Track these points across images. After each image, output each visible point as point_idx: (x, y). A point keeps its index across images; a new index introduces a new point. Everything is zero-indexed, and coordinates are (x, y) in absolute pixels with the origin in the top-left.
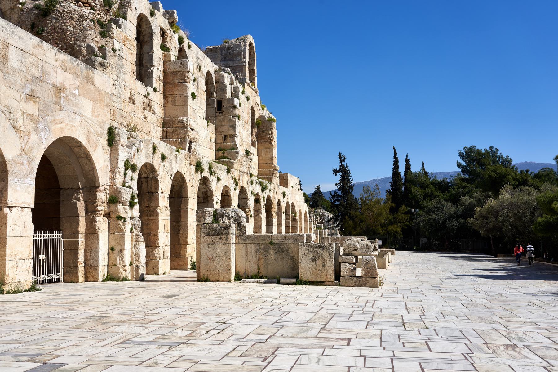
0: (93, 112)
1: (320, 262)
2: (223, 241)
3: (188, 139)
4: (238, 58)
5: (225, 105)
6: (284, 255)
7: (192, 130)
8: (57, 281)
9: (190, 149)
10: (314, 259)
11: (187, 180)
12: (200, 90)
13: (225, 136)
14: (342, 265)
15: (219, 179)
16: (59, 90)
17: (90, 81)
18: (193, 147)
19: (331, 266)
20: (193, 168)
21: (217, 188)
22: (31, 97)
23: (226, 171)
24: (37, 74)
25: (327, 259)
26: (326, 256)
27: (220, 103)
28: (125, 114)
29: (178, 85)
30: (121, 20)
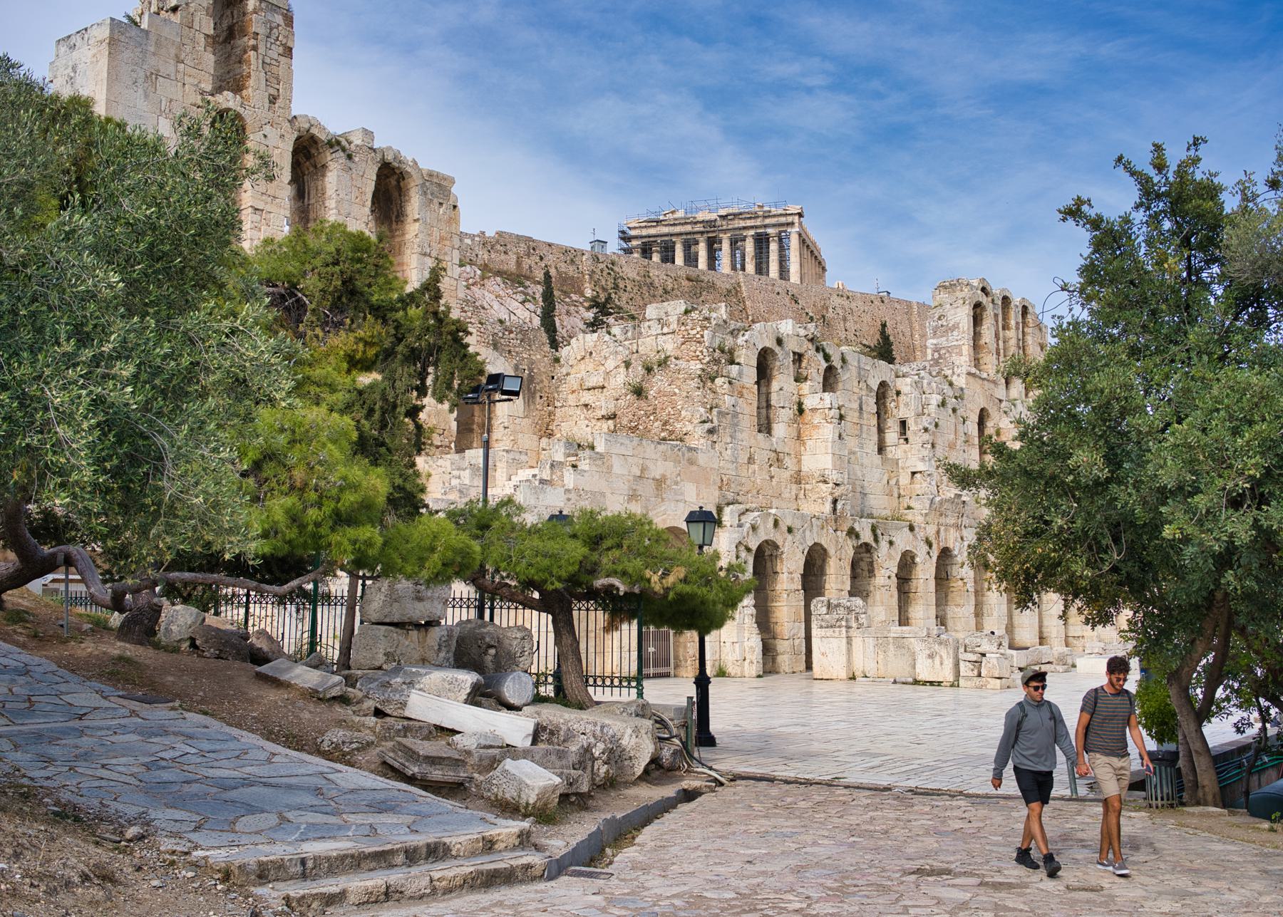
0: (698, 495)
1: (937, 660)
2: (837, 634)
3: (830, 499)
4: (955, 333)
5: (911, 424)
6: (904, 651)
7: (837, 485)
8: (667, 675)
9: (835, 510)
10: (931, 656)
11: (831, 551)
12: (865, 416)
13: (914, 473)
14: (962, 664)
15: (891, 543)
16: (660, 483)
17: (691, 462)
18: (839, 506)
19: (949, 663)
20: (842, 535)
21: (890, 557)
22: (633, 497)
23: (907, 529)
24: (638, 473)
25: (945, 656)
26: (943, 652)
27: (903, 424)
28: (744, 480)
29: (817, 427)
30: (735, 368)
